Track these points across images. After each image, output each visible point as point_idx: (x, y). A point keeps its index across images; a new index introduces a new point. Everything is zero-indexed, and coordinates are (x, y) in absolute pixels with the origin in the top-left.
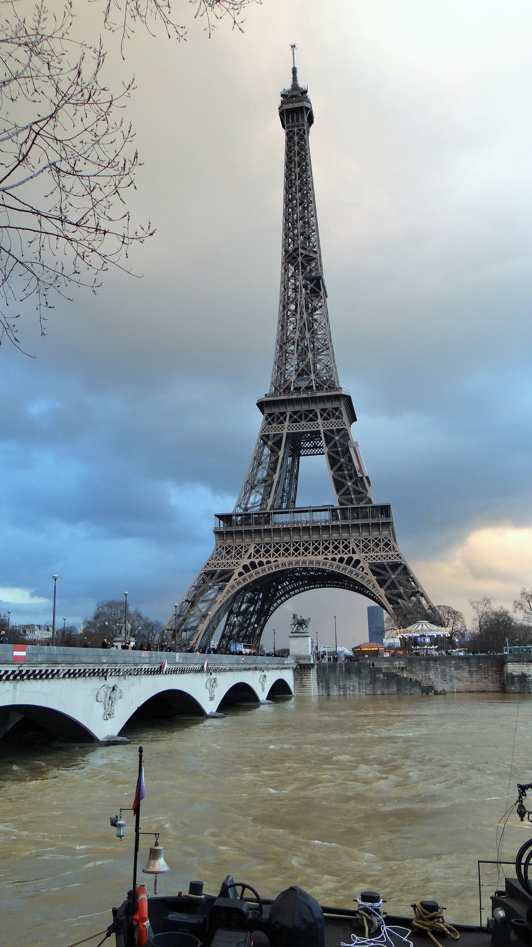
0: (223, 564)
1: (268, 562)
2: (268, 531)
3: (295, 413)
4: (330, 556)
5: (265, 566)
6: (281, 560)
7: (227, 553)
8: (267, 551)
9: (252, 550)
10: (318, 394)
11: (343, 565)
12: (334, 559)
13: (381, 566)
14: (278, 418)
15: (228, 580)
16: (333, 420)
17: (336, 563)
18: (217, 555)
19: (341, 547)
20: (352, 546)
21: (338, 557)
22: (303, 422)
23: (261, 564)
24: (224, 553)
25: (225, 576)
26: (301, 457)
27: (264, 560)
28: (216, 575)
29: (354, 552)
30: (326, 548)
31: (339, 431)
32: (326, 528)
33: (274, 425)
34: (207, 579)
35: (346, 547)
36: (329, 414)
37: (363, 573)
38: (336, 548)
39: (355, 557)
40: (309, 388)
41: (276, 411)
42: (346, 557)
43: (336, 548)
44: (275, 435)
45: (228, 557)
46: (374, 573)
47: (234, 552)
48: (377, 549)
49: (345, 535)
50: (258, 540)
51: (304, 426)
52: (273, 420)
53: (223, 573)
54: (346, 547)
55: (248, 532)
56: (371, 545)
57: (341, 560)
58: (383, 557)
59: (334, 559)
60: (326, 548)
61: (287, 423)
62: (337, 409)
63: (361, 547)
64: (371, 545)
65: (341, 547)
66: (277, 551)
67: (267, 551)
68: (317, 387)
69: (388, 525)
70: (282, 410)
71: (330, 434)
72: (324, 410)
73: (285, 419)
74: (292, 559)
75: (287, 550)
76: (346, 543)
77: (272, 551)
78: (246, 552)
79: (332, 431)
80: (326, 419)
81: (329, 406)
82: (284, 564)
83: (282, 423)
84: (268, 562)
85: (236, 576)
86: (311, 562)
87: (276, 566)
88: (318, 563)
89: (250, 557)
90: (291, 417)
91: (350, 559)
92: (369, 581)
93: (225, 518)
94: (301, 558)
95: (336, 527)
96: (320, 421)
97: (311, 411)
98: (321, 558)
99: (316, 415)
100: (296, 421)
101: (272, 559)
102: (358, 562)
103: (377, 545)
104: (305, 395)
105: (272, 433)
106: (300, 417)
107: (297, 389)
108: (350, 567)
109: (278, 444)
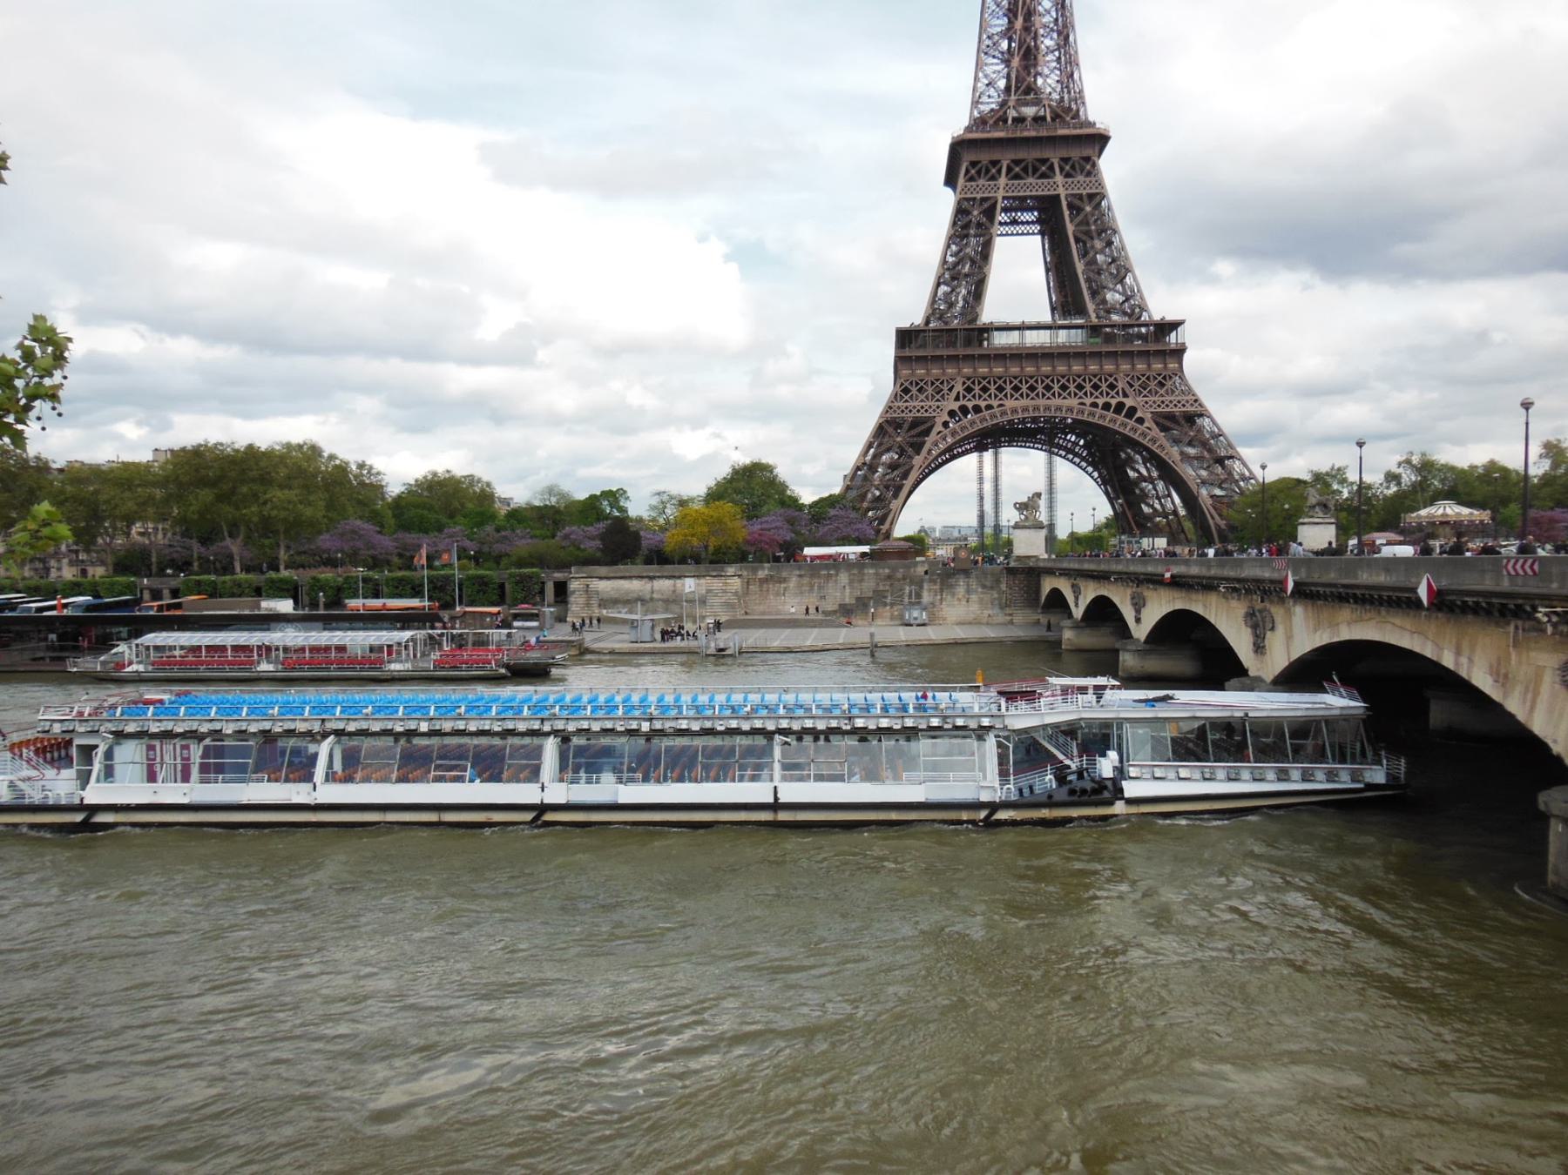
0: (917, 406)
1: (989, 407)
2: (986, 358)
3: (1017, 162)
4: (1088, 401)
5: (986, 413)
6: (1010, 403)
7: (920, 390)
8: (984, 389)
9: (959, 388)
10: (1061, 132)
11: (1110, 414)
12: (1095, 405)
13: (1171, 417)
14: (988, 171)
15: (927, 432)
16: (1081, 178)
17: (1099, 411)
18: (903, 390)
19: (1104, 387)
20: (1120, 385)
21: (1100, 402)
22: (1031, 180)
23: (977, 409)
24: (914, 390)
25: (920, 428)
26: (1039, 237)
27: (983, 404)
28: (906, 426)
29: (1125, 395)
30: (1080, 387)
31: (1091, 197)
32: (1080, 355)
33: (981, 182)
34: (890, 430)
35: (1112, 386)
36: (1073, 167)
37: (1141, 428)
38: (1096, 387)
39: (1129, 402)
40: (1038, 119)
41: (985, 157)
42: (1114, 402)
43: (1096, 387)
44: (984, 200)
45: (922, 397)
46: (1164, 429)
47: (930, 390)
48: (1162, 392)
49: (1109, 367)
50: (967, 371)
51: (1033, 187)
52: (979, 172)
53: (916, 423)
54: (1112, 386)
55: (953, 359)
56: (1153, 385)
57: (1107, 406)
58: (1172, 404)
59: (1095, 405)
60: (1080, 387)
61: (1003, 180)
62: (1087, 159)
63: (1136, 385)
64: (1153, 385)
65: (1104, 387)
66: (1000, 389)
67: (984, 389)
68: (1053, 119)
69: (1179, 352)
70: (995, 157)
71: (1077, 202)
72: (1065, 160)
73: (999, 171)
74: (1024, 402)
75: (1016, 389)
76: (1111, 380)
77: (993, 389)
78: (950, 389)
79: (1080, 197)
80: (1068, 175)
81: (1075, 153)
82: (1014, 411)
83: (993, 178)
84: (989, 407)
85: (938, 427)
86: (1059, 409)
87: (1004, 413)
88: (1070, 410)
89: (957, 399)
90: (1009, 170)
91: (1120, 406)
92: (1154, 440)
93: (905, 337)
94: (1041, 402)
95: (1097, 355)
96: (1059, 178)
97: (1044, 161)
98: (1073, 402)
99: (1051, 168)
100: (1017, 177)
101: (995, 403)
102: (1133, 410)
103: (1161, 385)
104: (1033, 134)
105: (979, 196)
106: (1025, 170)
107: (1020, 120)
108: (1121, 418)
109: (990, 213)
